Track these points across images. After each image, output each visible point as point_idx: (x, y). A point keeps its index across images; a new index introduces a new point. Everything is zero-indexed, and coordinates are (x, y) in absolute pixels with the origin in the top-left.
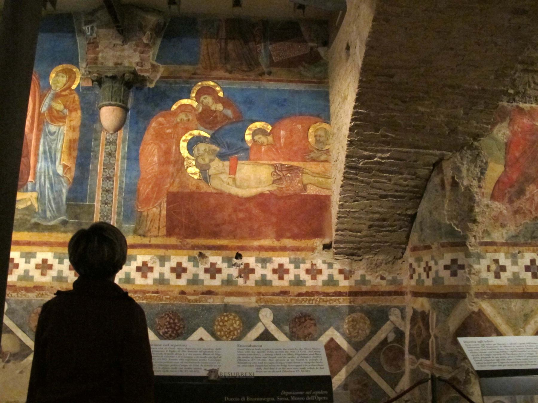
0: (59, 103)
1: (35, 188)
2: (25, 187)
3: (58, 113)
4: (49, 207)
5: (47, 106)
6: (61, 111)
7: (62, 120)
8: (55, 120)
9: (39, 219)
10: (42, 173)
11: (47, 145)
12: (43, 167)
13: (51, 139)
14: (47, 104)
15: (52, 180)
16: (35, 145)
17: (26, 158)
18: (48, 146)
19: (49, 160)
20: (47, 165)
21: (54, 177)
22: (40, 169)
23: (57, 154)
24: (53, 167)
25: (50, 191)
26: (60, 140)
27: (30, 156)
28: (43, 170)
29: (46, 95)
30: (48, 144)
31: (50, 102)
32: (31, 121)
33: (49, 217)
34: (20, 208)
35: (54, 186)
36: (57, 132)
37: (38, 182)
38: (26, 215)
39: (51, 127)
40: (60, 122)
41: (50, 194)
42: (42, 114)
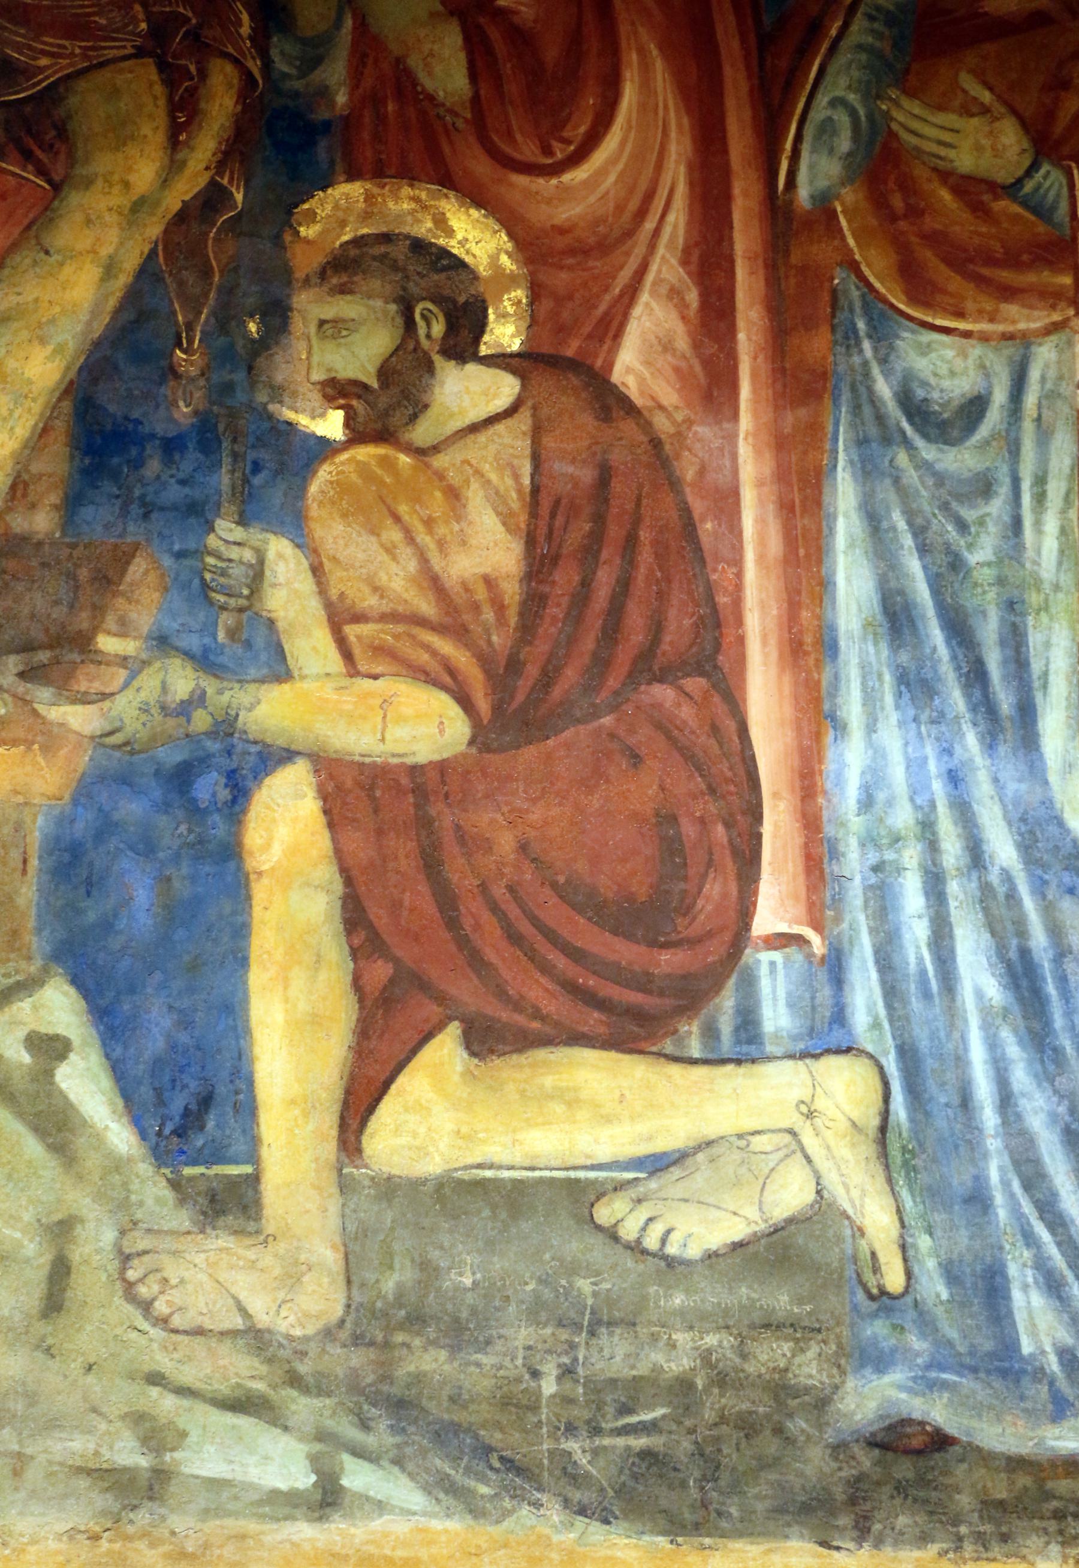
0: (970, 108)
1: (840, 1017)
2: (727, 1002)
3: (979, 209)
4: (1029, 1238)
5: (844, 144)
6: (1012, 189)
7: (1030, 278)
8: (955, 283)
9: (934, 1386)
10: (896, 839)
11: (908, 541)
12: (898, 774)
13: (940, 479)
14: (842, 118)
15: (1022, 931)
16: (775, 546)
17: (695, 684)
18: (923, 549)
19: (956, 699)
20: (948, 752)
21: (1040, 889)
22: (867, 803)
23: (1035, 639)
24: (1012, 787)
25: (1013, 1050)
26: (1040, 480)
27: (741, 660)
28: (903, 817)
29: (815, 29)
30: (919, 532)
31: (872, 93)
32: (693, 297)
33: (1053, 1364)
34: (694, 1252)
35: (1051, 989)
36: (1000, 397)
37: (865, 946)
38: (771, 1326)
39: (925, 350)
40: (1009, 293)
41: (1021, 1077)
42: (808, 223)
